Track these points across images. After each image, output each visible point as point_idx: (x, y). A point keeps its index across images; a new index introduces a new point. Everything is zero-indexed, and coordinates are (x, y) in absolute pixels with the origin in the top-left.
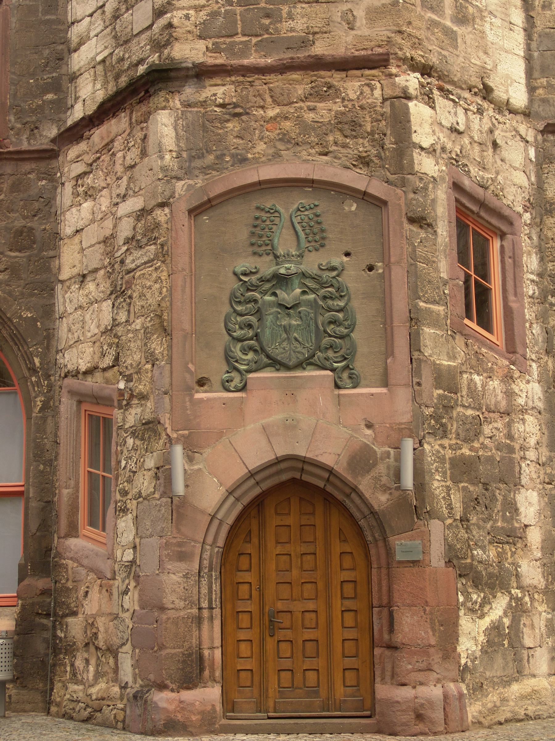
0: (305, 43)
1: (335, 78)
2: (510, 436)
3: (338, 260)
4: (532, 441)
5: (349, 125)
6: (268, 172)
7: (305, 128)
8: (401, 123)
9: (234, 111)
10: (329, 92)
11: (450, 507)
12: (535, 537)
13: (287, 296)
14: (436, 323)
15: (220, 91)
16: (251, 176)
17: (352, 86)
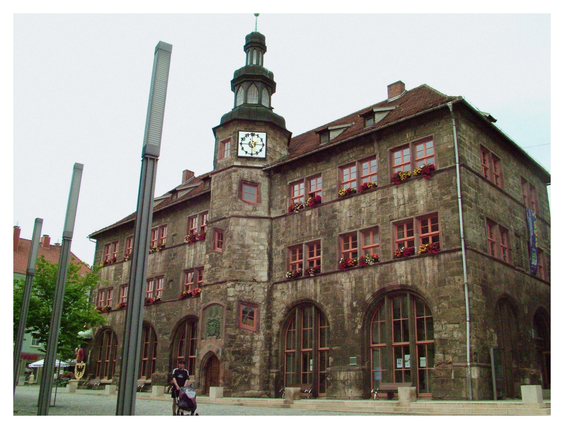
0: (218, 279)
1: (219, 285)
2: (251, 345)
3: (219, 317)
4: (259, 346)
5: (221, 293)
6: (212, 302)
7: (216, 294)
8: (226, 292)
9: (209, 292)
10: (219, 288)
11: (231, 359)
12: (257, 365)
13: (212, 323)
14: (231, 327)
15: (207, 289)
16: (210, 303)
17: (222, 286)
